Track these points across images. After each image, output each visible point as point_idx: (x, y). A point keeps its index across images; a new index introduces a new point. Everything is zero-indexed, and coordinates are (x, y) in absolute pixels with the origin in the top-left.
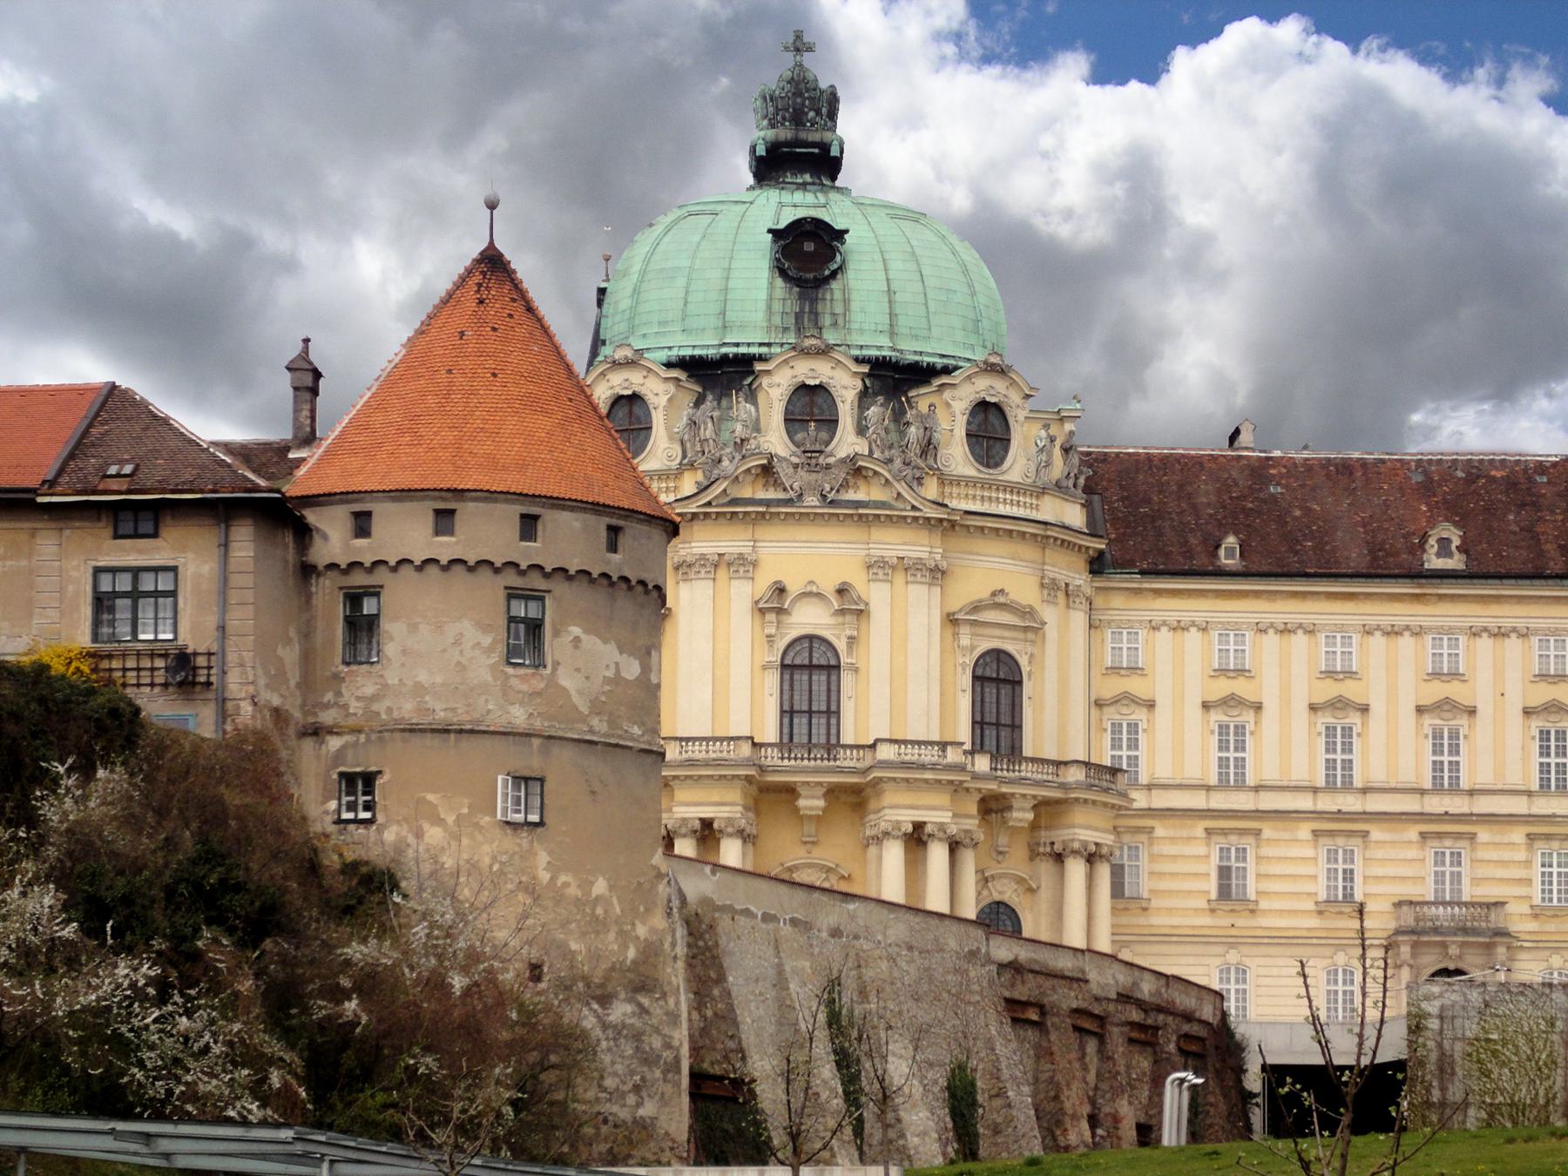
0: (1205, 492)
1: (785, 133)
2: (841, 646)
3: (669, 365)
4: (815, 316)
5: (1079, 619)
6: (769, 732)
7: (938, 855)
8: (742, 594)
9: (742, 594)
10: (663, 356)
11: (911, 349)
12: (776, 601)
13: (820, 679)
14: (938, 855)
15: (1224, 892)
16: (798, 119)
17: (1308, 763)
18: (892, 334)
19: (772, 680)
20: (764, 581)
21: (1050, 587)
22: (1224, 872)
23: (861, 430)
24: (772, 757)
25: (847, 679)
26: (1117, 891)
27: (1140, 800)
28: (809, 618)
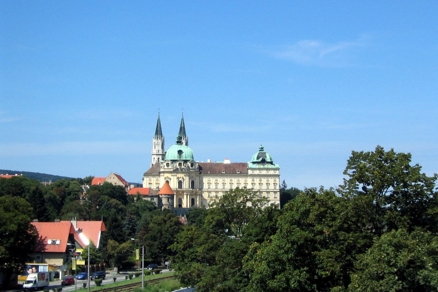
0: (208, 167)
1: (178, 140)
2: (182, 181)
3: (171, 160)
4: (180, 157)
5: (199, 177)
6: (177, 187)
7: (189, 196)
8: (175, 177)
9: (175, 177)
10: (170, 160)
11: (187, 159)
12: (178, 178)
13: (181, 183)
14: (189, 196)
15: (208, 196)
16: (179, 139)
17: (214, 187)
18: (186, 158)
19: (177, 184)
20: (177, 177)
21: (196, 176)
22: (208, 195)
23: (184, 166)
24: (178, 189)
25: (183, 183)
26: (201, 196)
27: (203, 190)
28: (180, 179)
